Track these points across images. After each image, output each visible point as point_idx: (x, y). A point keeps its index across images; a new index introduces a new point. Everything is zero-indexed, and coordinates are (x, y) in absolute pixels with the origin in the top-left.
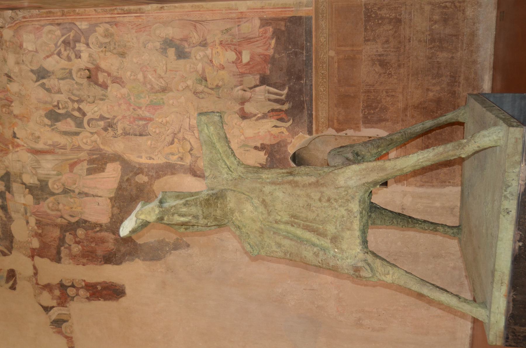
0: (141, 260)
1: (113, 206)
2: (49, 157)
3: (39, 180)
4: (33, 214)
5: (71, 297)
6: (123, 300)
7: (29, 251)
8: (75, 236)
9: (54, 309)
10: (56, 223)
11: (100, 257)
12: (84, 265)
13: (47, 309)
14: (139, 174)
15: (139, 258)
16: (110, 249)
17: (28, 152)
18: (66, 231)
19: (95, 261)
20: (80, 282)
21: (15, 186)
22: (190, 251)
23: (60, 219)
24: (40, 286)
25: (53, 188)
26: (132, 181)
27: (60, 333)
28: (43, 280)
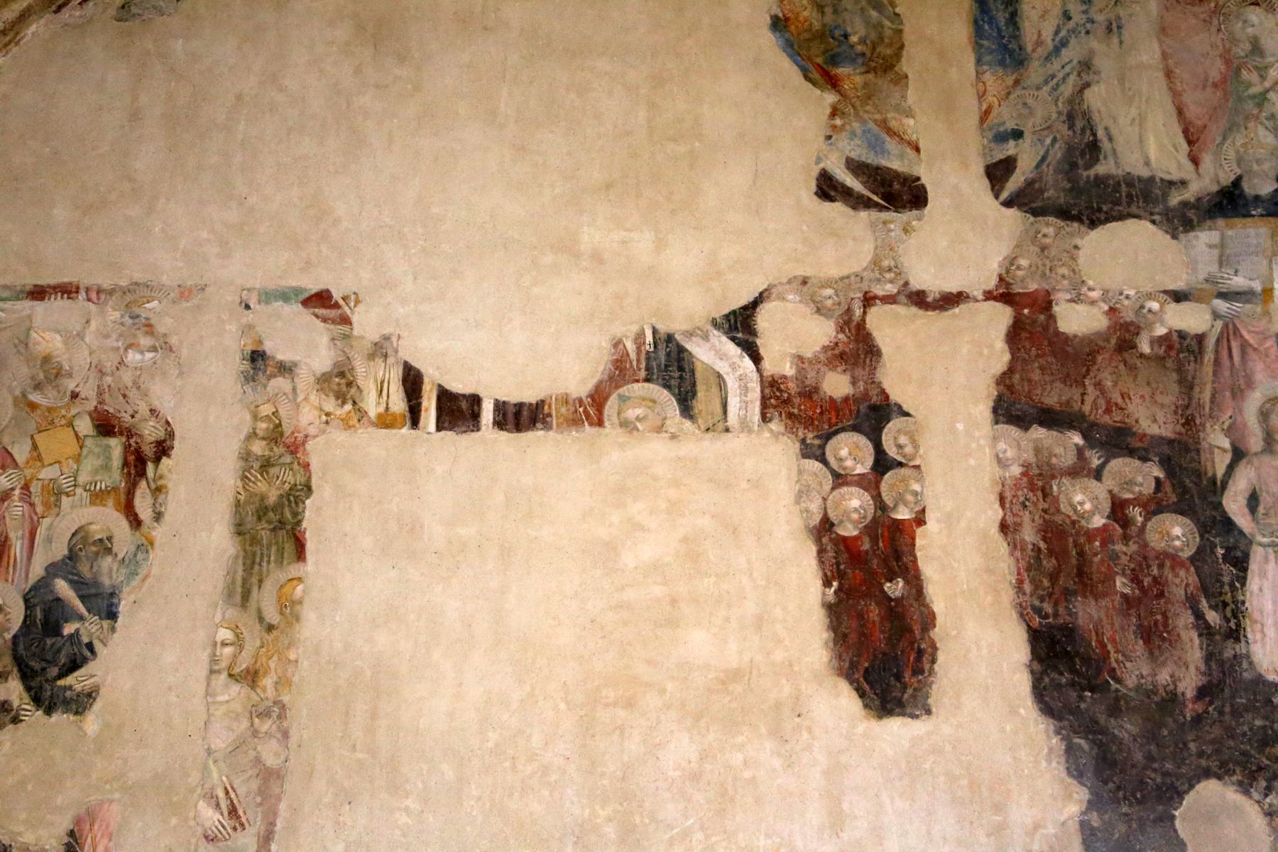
0: (1083, 813)
4: (1226, 326)
5: (822, 447)
7: (1032, 286)
8: (1154, 507)
9: (748, 363)
10: (1203, 425)
11: (1061, 610)
12: (1004, 527)
15: (1091, 805)
16: (1114, 665)
18: (1166, 462)
19: (1036, 585)
20: (910, 498)
23: (1226, 443)
24: (858, 312)
27: (620, 372)
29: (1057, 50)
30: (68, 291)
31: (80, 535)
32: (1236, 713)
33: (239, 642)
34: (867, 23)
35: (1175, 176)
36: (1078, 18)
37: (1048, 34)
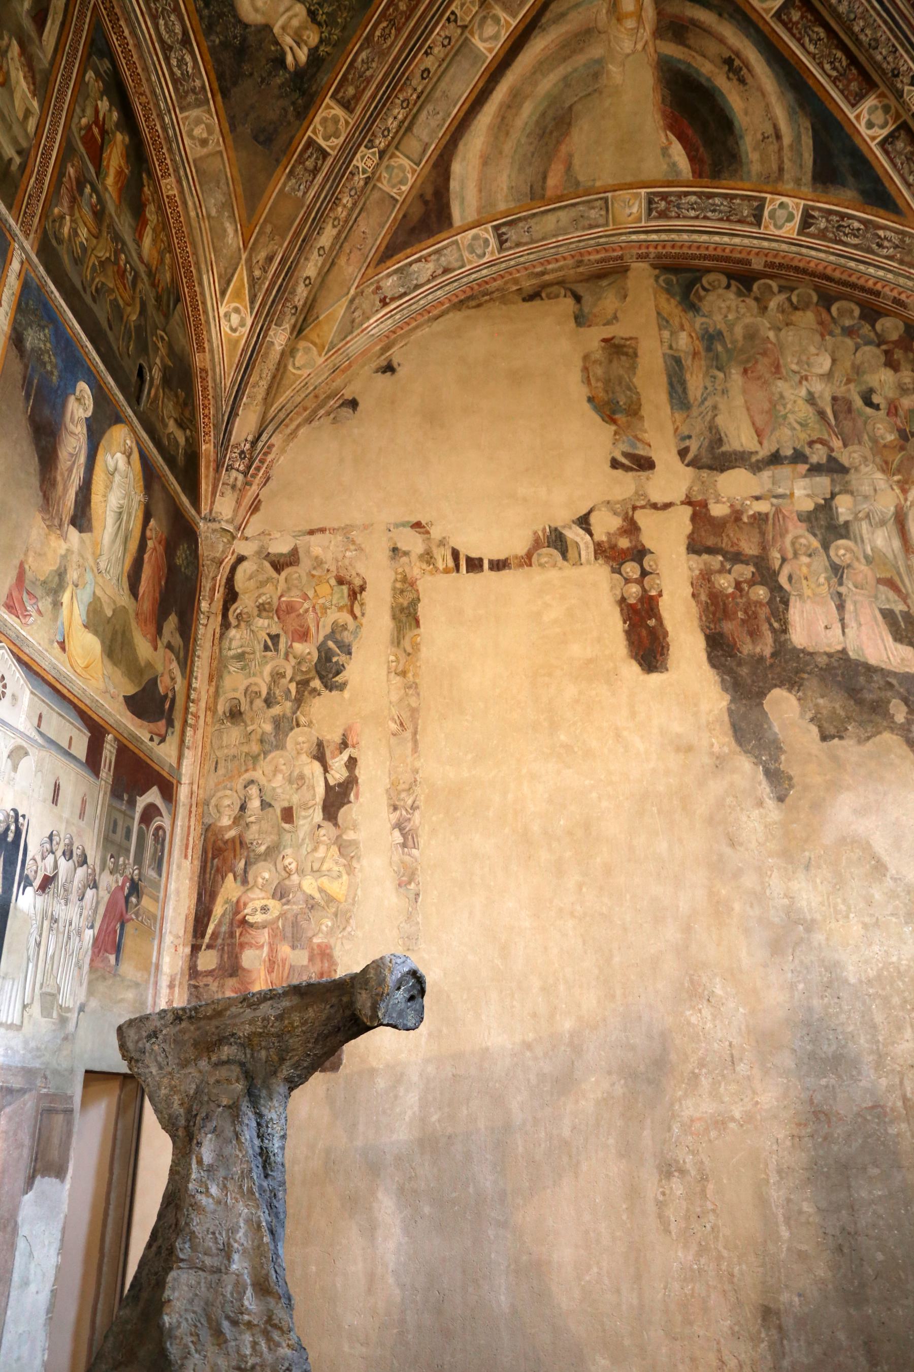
1: (830, 655)
2: (897, 544)
3: (847, 523)
6: (635, 667)
7: (699, 498)
8: (752, 583)
9: (588, 537)
12: (693, 595)
13: (584, 522)
14: (907, 704)
15: (731, 701)
17: (896, 507)
18: (756, 565)
19: (707, 617)
21: (823, 482)
22: (770, 803)
23: (778, 556)
24: (630, 513)
25: (838, 548)
26: (889, 694)
27: (537, 544)
28: (643, 519)
29: (703, 402)
30: (322, 530)
31: (335, 623)
32: (786, 662)
33: (397, 661)
35: (753, 450)
36: (710, 389)
37: (699, 394)
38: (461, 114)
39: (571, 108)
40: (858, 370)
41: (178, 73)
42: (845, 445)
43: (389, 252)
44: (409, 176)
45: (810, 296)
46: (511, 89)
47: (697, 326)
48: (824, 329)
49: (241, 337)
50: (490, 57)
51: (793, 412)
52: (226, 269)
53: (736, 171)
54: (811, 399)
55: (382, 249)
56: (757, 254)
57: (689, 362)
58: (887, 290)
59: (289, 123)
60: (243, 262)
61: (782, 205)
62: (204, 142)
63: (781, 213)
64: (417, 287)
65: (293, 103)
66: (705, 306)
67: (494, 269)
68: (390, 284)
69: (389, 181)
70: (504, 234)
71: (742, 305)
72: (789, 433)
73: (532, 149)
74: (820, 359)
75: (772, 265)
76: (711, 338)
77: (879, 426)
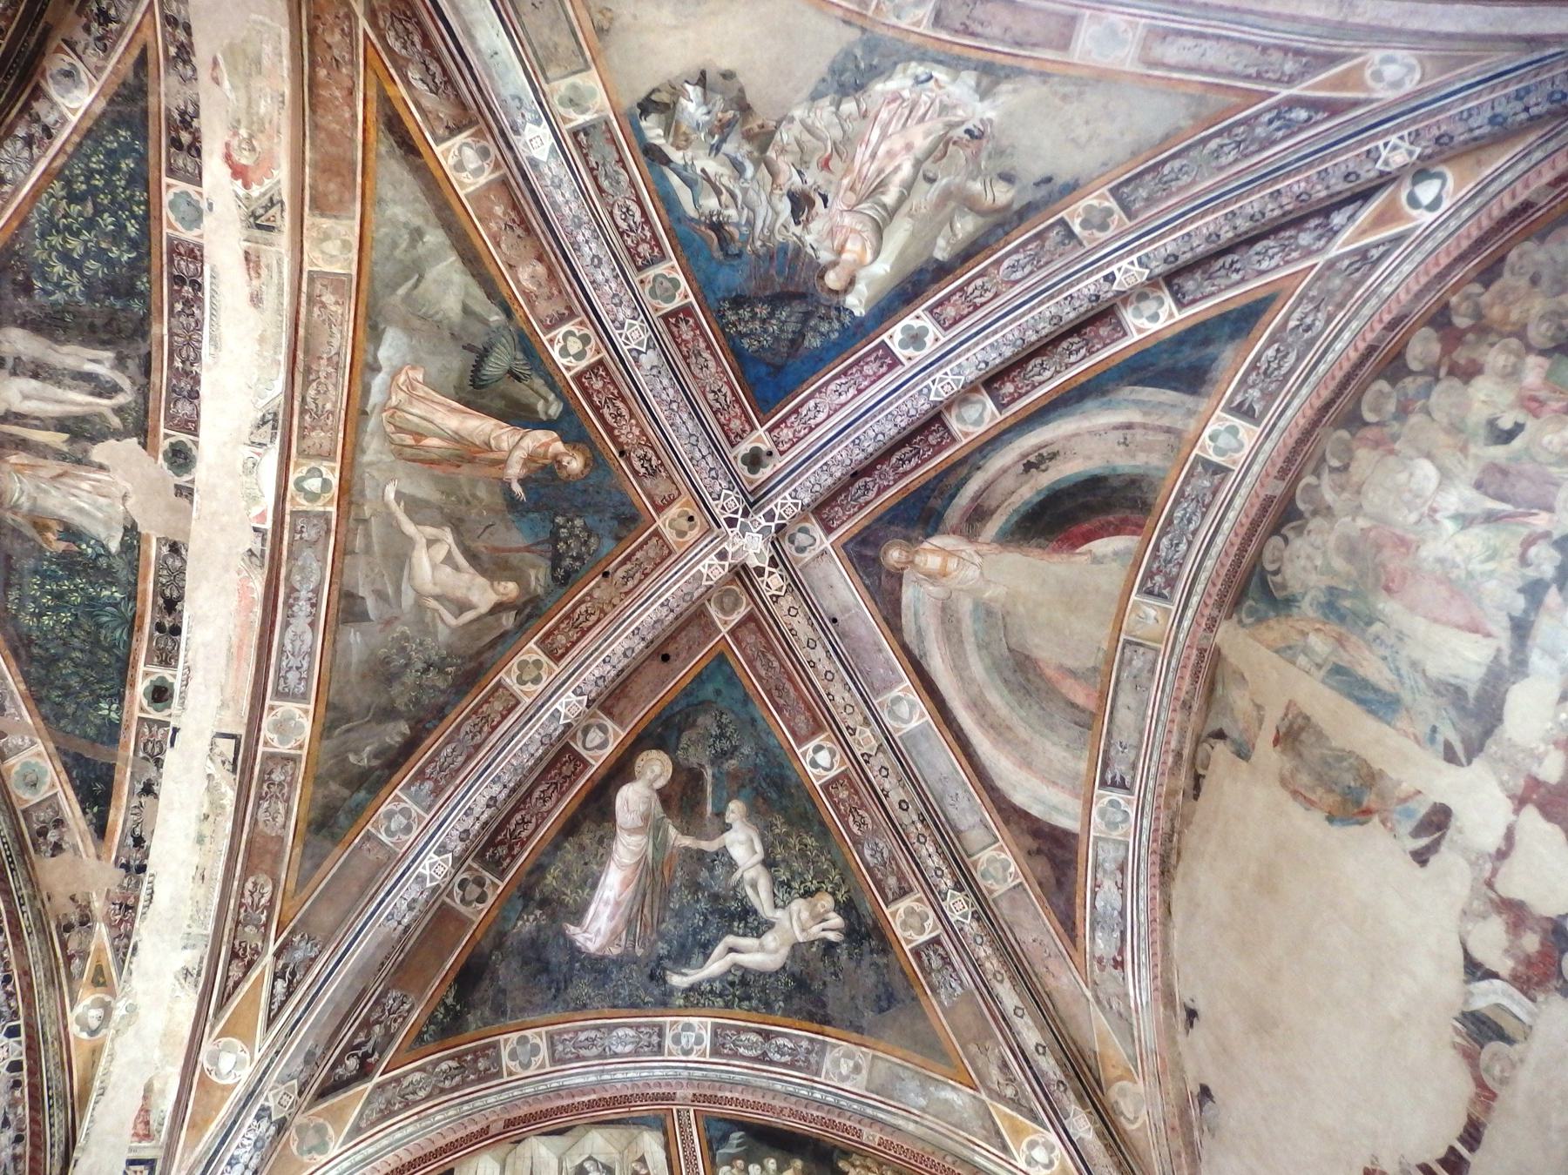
7: (1521, 782)
9: (1496, 982)
13: (1475, 970)
24: (1493, 895)
27: (1471, 1058)
29: (1399, 675)
34: (1348, 770)
38: (969, 770)
39: (1010, 650)
40: (1456, 428)
41: (787, 1058)
42: (1550, 509)
43: (1068, 925)
44: (1003, 856)
45: (1339, 439)
46: (967, 707)
47: (1311, 613)
48: (1384, 445)
49: (1063, 1163)
50: (928, 717)
51: (1468, 559)
52: (984, 1127)
53: (1151, 483)
54: (1465, 520)
55: (1061, 931)
56: (1262, 485)
57: (1346, 657)
58: (1370, 337)
59: (887, 966)
60: (988, 1101)
61: (1212, 438)
62: (857, 1069)
63: (1222, 442)
64: (1122, 914)
65: (872, 952)
66: (1295, 587)
67: (1147, 809)
68: (1102, 944)
69: (997, 882)
70: (1114, 778)
71: (1313, 537)
72: (1491, 585)
73: (1036, 707)
74: (1419, 473)
75: (1283, 473)
76: (1331, 607)
77: (1546, 439)
